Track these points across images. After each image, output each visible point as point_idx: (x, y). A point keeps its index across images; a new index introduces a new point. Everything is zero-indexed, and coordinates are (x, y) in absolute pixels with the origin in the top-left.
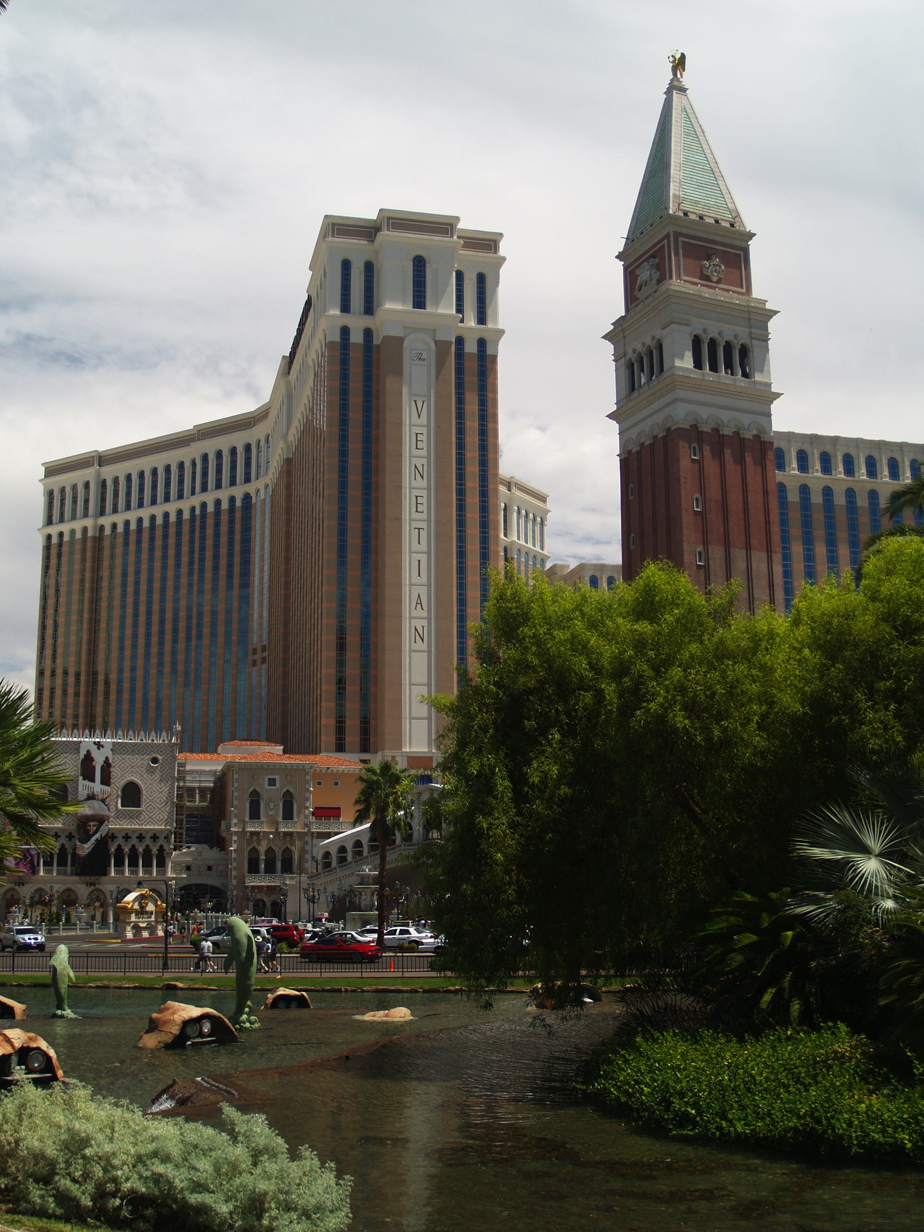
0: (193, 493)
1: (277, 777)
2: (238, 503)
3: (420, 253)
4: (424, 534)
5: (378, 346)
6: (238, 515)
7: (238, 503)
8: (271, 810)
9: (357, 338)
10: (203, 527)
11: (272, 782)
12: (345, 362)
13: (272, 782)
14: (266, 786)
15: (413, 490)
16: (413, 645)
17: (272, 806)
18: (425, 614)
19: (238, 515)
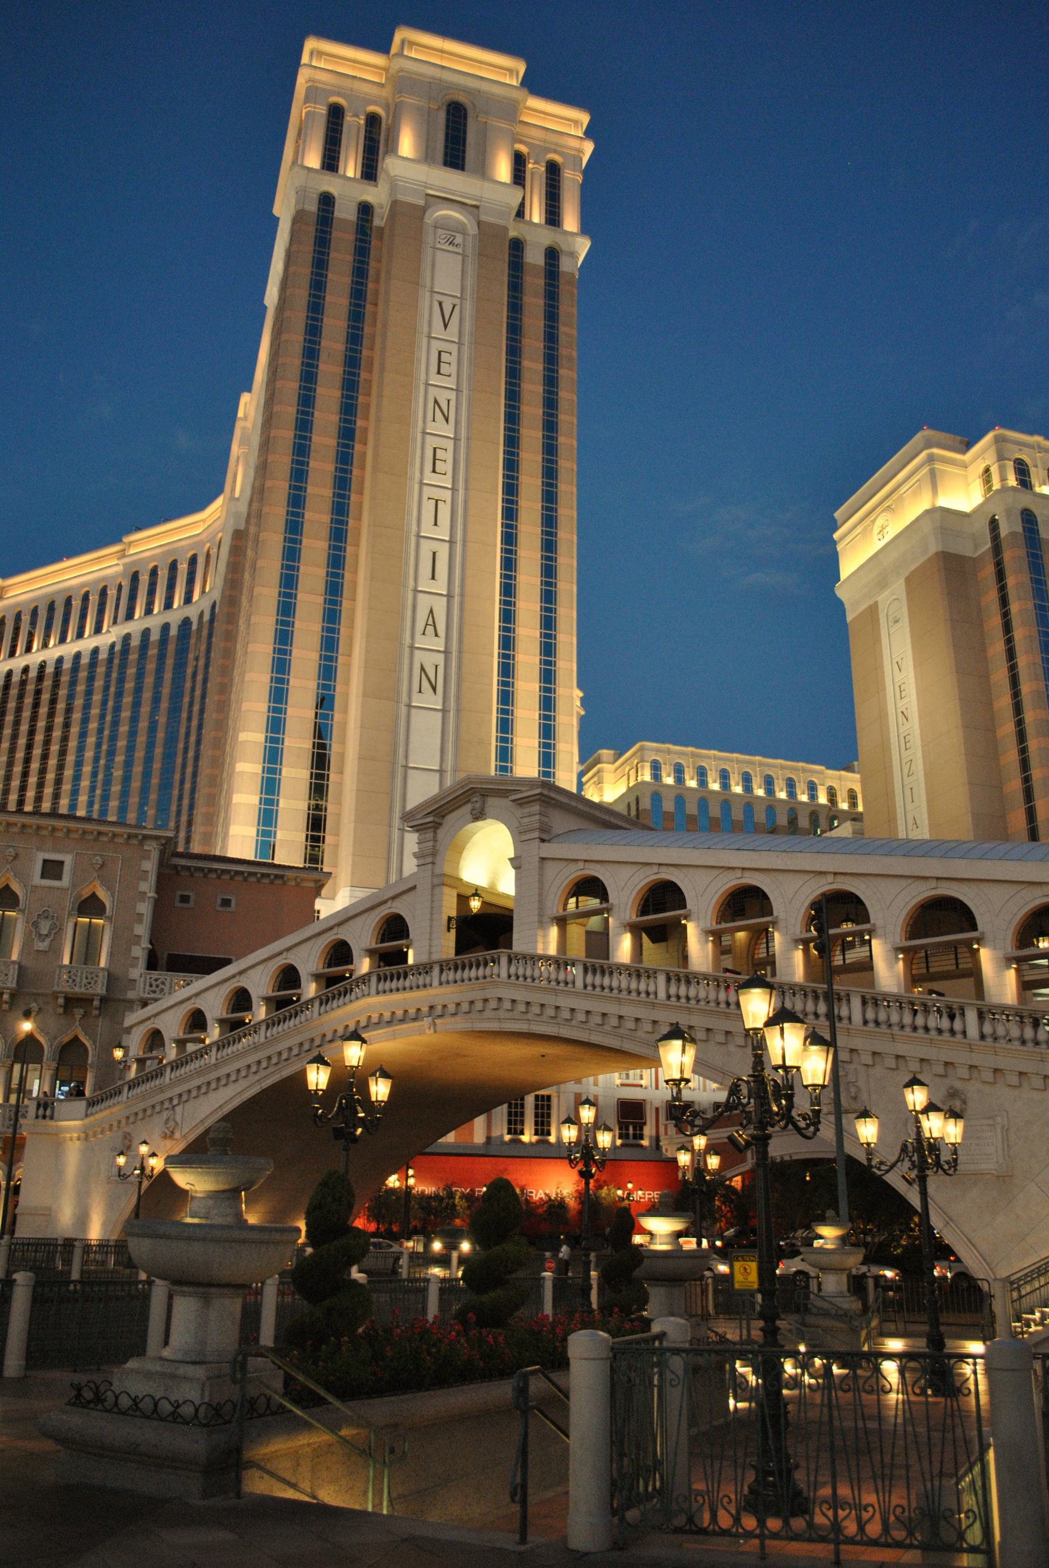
0: (115, 622)
1: (68, 859)
2: (173, 632)
3: (462, 98)
4: (445, 511)
5: (381, 230)
6: (171, 648)
7: (173, 632)
8: (42, 938)
9: (345, 212)
10: (123, 666)
11: (52, 870)
12: (323, 242)
13: (52, 870)
14: (37, 880)
15: (425, 488)
16: (415, 695)
17: (45, 927)
18: (439, 644)
19: (171, 648)
